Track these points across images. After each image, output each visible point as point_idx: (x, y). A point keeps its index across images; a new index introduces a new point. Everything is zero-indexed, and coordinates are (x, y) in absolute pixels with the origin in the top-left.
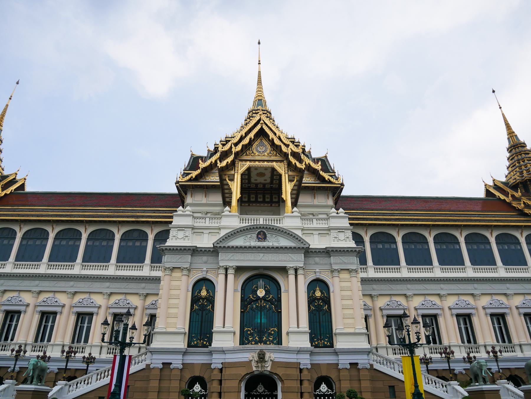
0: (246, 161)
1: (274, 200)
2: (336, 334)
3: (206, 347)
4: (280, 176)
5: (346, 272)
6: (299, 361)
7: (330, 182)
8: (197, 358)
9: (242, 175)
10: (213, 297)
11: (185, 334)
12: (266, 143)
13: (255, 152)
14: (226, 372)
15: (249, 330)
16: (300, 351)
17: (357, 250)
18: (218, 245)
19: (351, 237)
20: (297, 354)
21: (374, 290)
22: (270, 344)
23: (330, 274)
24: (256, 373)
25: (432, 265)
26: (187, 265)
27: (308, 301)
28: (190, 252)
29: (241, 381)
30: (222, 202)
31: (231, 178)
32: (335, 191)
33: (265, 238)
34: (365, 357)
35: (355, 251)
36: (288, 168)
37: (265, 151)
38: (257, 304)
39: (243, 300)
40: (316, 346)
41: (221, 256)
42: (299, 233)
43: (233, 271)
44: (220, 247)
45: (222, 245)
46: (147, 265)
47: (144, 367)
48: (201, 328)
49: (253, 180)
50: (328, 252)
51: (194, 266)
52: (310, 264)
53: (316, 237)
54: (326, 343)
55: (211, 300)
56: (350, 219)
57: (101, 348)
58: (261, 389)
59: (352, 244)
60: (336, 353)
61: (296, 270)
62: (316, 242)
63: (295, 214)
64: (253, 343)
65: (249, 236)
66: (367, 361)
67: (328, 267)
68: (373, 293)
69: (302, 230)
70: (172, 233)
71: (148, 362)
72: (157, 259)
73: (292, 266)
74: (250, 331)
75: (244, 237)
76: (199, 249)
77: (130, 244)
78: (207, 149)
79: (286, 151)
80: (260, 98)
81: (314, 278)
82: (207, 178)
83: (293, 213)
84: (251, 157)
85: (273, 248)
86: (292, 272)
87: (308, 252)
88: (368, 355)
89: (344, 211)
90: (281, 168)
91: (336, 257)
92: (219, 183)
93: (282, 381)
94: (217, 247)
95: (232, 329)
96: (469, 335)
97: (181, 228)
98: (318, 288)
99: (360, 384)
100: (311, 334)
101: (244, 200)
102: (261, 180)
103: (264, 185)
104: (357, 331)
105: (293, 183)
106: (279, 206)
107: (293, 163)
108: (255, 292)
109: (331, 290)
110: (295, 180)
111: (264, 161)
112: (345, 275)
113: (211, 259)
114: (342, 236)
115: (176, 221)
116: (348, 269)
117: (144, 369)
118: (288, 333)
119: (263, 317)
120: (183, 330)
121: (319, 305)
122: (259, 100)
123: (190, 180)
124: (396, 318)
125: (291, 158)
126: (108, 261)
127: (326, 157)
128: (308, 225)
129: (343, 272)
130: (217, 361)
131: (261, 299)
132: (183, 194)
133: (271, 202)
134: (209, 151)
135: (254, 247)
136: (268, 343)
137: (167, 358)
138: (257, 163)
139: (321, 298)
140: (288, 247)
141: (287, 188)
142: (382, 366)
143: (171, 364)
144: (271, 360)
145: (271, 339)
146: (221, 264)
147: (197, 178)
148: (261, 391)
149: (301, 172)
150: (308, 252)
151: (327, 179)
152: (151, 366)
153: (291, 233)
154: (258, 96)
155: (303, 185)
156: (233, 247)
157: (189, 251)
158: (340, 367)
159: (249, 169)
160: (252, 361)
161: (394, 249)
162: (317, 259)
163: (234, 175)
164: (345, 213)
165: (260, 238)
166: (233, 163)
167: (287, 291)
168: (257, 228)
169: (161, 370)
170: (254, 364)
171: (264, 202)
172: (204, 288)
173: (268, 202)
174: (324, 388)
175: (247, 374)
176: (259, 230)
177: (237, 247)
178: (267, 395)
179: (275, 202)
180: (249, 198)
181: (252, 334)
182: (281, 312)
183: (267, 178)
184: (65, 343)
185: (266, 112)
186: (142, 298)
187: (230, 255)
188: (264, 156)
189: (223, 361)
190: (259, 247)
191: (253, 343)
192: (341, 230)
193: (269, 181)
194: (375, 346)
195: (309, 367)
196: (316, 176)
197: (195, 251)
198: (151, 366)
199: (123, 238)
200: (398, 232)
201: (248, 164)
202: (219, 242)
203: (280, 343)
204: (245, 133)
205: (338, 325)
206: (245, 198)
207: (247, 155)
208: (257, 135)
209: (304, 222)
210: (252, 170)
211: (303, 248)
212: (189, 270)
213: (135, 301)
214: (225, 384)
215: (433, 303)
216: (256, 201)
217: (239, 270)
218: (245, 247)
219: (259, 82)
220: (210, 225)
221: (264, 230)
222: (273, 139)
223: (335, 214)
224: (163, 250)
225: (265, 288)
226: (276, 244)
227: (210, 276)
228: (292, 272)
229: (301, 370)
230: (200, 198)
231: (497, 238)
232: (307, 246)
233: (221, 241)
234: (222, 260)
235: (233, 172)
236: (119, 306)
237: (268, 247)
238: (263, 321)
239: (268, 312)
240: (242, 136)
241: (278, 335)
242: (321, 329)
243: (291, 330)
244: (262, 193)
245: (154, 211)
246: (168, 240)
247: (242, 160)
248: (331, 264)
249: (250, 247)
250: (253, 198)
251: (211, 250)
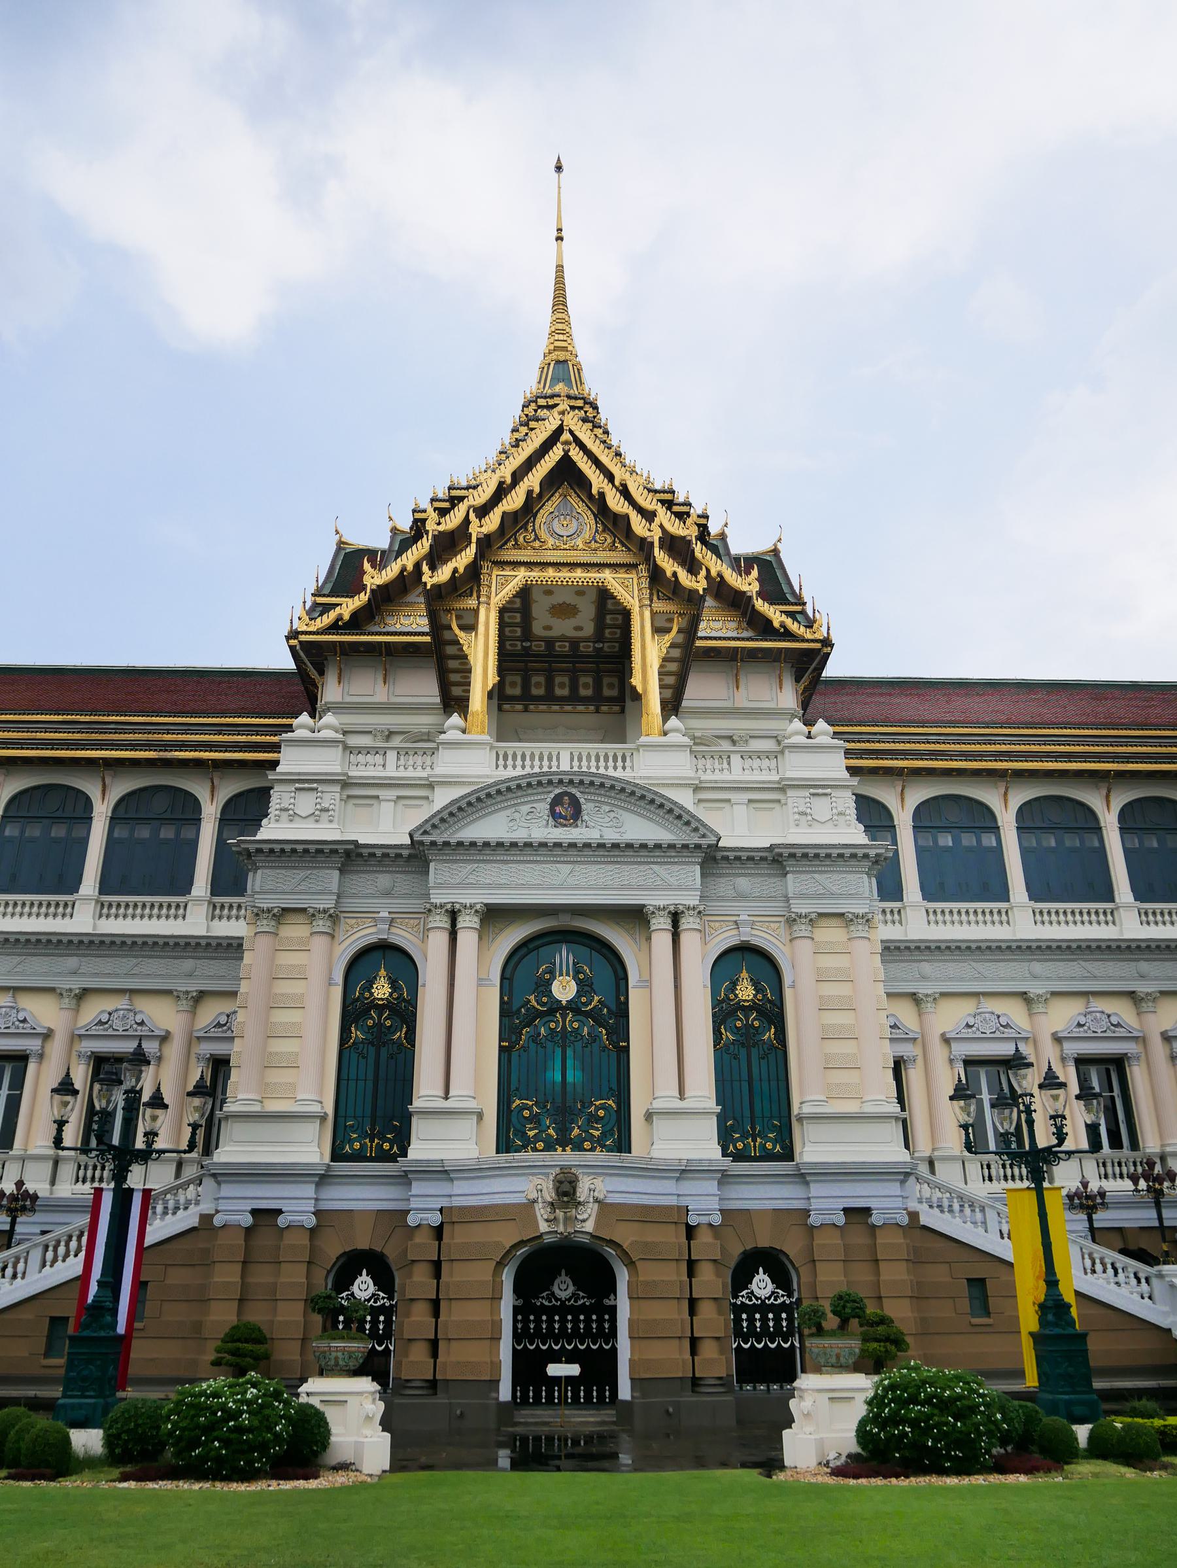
0: (516, 564)
1: (607, 692)
2: (800, 1119)
3: (392, 1158)
4: (626, 614)
5: (834, 922)
6: (684, 1202)
7: (787, 635)
8: (362, 1195)
9: (502, 611)
10: (412, 1003)
11: (323, 1118)
12: (581, 508)
13: (544, 535)
14: (456, 1238)
15: (526, 1107)
16: (685, 1172)
17: (872, 853)
18: (427, 839)
19: (853, 812)
20: (678, 1179)
21: (924, 978)
22: (593, 1149)
23: (782, 930)
24: (548, 1239)
26: (328, 902)
27: (714, 1015)
28: (338, 860)
29: (500, 1265)
30: (438, 700)
31: (468, 620)
32: (806, 662)
33: (576, 814)
34: (894, 1188)
35: (866, 856)
36: (651, 589)
37: (577, 533)
38: (553, 1025)
39: (506, 1011)
40: (739, 1157)
41: (437, 872)
42: (685, 799)
43: (476, 919)
44: (433, 843)
45: (438, 837)
46: (198, 900)
47: (194, 1222)
48: (375, 1100)
49: (537, 629)
50: (777, 860)
51: (349, 904)
52: (722, 899)
53: (741, 811)
54: (769, 1145)
55: (404, 1012)
56: (848, 753)
57: (56, 1162)
58: (564, 1289)
59: (855, 834)
60: (802, 1177)
61: (675, 917)
62: (739, 829)
63: (674, 738)
64: (540, 1145)
65: (525, 809)
66: (899, 1203)
67: (777, 907)
68: (923, 989)
69: (697, 789)
70: (279, 798)
71: (206, 1207)
72: (230, 880)
73: (662, 903)
74: (529, 1108)
75: (508, 812)
76: (365, 852)
77: (144, 832)
78: (390, 525)
79: (647, 534)
80: (562, 356)
81: (734, 942)
82: (390, 621)
83: (665, 734)
84: (530, 552)
85: (601, 846)
86: (661, 923)
87: (714, 859)
88: (903, 1182)
89: (831, 729)
90: (629, 590)
91: (804, 877)
92: (428, 639)
93: (630, 1264)
94: (421, 843)
95: (472, 1104)
97: (306, 783)
98: (744, 974)
99: (878, 1273)
100: (721, 1119)
101: (509, 691)
102: (563, 628)
103: (575, 643)
104: (869, 1109)
105: (668, 639)
106: (623, 711)
107: (669, 574)
108: (543, 987)
109: (787, 980)
110: (675, 629)
111: (572, 566)
112: (830, 933)
113: (403, 882)
114: (821, 809)
115: (291, 761)
116: (843, 914)
117: (193, 1229)
118: (649, 1116)
119: (569, 1063)
120: (315, 1108)
121: (748, 1026)
122: (558, 362)
123: (334, 627)
124: (993, 1069)
125: (662, 559)
126: (74, 888)
127: (775, 552)
128: (714, 774)
129: (824, 922)
130: (425, 1204)
131: (565, 1008)
132: (314, 673)
133: (597, 700)
134: (394, 531)
135: (543, 845)
136: (587, 1145)
137: (266, 1195)
138: (551, 572)
139: (754, 1007)
140: (651, 844)
141: (649, 655)
142: (947, 1215)
143: (279, 1212)
144: (596, 1200)
145: (596, 1133)
146: (436, 899)
147: (357, 621)
148: (563, 1295)
149: (693, 600)
150: (714, 859)
151: (776, 624)
152: (218, 1221)
153: (658, 801)
154: (556, 349)
155: (698, 643)
156: (473, 844)
157: (336, 858)
158: (814, 1220)
159: (525, 593)
160: (535, 1201)
161: (990, 849)
162: (743, 883)
163: (476, 612)
164: (836, 735)
165: (561, 816)
166: (474, 573)
167: (647, 984)
168: (550, 782)
169: (248, 1230)
170: (541, 1212)
171: (574, 698)
172: (383, 972)
173: (585, 700)
174: (762, 1285)
175: (521, 1243)
176: (557, 791)
177: (486, 844)
178: (583, 1309)
180: (526, 685)
181: (535, 1119)
182: (627, 1049)
183: (584, 623)
185: (580, 403)
186: (185, 1004)
187: (464, 870)
188: (574, 548)
189: (445, 1202)
190: (558, 845)
191: (540, 1145)
192: (818, 788)
193: (589, 629)
194: (927, 1154)
195: (717, 1219)
196: (744, 615)
197: (351, 857)
198: (218, 1221)
199: (121, 813)
200: (1006, 794)
201: (521, 576)
202: (428, 827)
203: (623, 1145)
204: (514, 475)
205: (807, 1091)
206: (513, 684)
207: (517, 546)
208: (552, 481)
209: (701, 762)
210: (536, 595)
211: (698, 847)
212: (334, 918)
213: (163, 1015)
214: (453, 1275)
215: (1114, 1020)
216: (550, 698)
217: (494, 916)
218: (514, 845)
219: (560, 301)
220: (402, 773)
221: (574, 791)
222: (602, 495)
223: (802, 740)
224: (249, 855)
225: (577, 972)
226: (611, 836)
227: (402, 937)
228: (661, 923)
229: (690, 1231)
230: (366, 686)
232: (712, 840)
233: (434, 826)
234: (440, 886)
235: (472, 602)
236: (110, 1032)
237: (587, 845)
238: (570, 1079)
239: (587, 1050)
240: (501, 484)
241: (619, 1120)
242: (756, 1102)
243: (658, 1105)
244: (569, 672)
245: (220, 729)
246: (264, 822)
247: (502, 564)
249: (528, 845)
250: (538, 685)
251: (405, 853)
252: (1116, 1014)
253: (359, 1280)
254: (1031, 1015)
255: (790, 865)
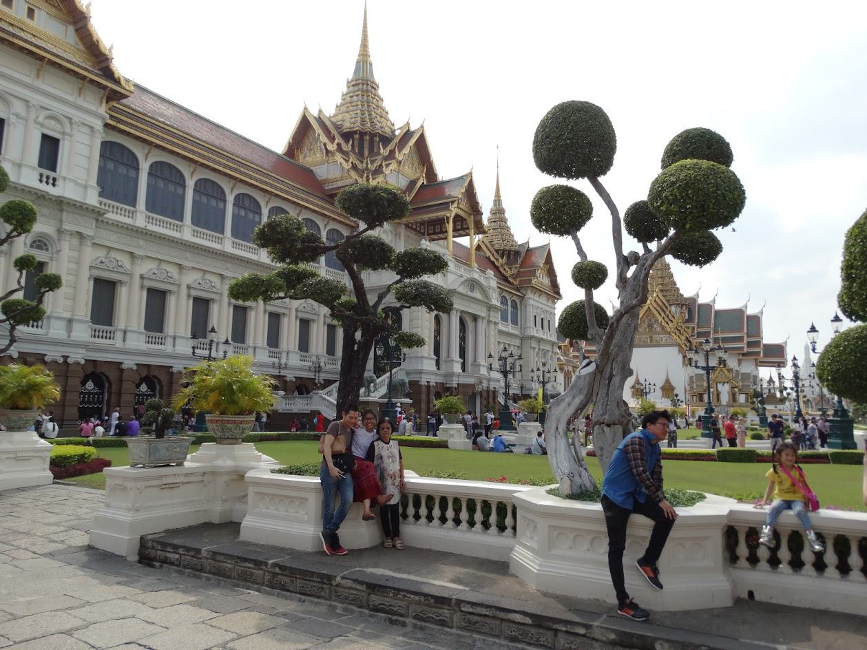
21: (228, 269)
25: (182, 221)
68: (138, 252)
96: (155, 320)
178: (96, 394)
179: (421, 233)
184: (258, 345)
194: (123, 328)
231: (238, 197)
248: (489, 316)
252: (121, 261)
253: (88, 383)
254: (222, 283)
255: (492, 309)
